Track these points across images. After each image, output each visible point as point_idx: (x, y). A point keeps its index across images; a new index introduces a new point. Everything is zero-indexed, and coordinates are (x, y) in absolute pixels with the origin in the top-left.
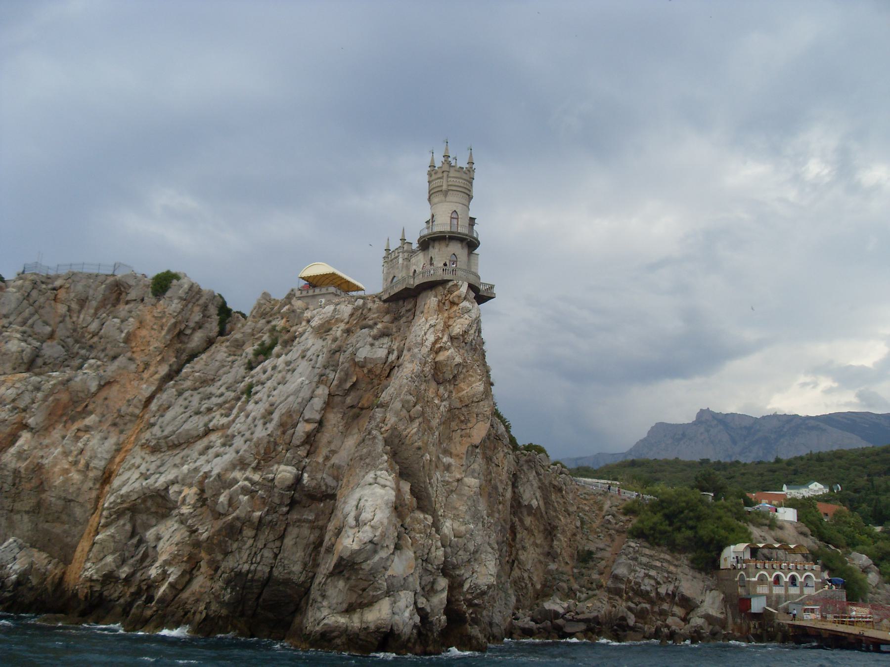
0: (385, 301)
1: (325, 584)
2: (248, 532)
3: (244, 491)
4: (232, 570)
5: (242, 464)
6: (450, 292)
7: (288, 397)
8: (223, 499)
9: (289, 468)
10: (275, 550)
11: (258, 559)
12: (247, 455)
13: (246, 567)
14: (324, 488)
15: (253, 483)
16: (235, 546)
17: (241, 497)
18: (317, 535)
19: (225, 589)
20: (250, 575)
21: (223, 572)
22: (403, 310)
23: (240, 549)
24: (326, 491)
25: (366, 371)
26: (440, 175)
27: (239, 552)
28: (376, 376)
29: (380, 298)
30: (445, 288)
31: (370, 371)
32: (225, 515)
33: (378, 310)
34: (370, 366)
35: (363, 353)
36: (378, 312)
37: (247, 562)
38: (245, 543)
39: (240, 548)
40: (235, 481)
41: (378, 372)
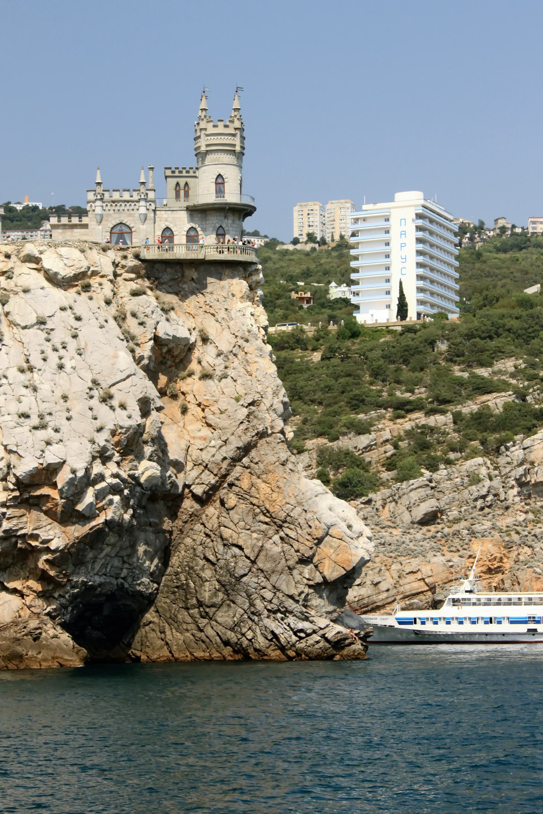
0: (143, 261)
1: (308, 595)
2: (112, 539)
3: (114, 490)
4: (84, 583)
5: (103, 456)
6: (250, 275)
7: (128, 377)
8: (89, 497)
9: (155, 464)
10: (125, 559)
11: (108, 570)
12: (110, 446)
13: (98, 580)
14: (168, 487)
15: (123, 480)
16: (90, 555)
17: (111, 497)
18: (162, 540)
19: (66, 608)
20: (99, 589)
21: (73, 587)
22: (166, 277)
23: (95, 560)
24: (170, 490)
25: (165, 350)
26: (233, 132)
27: (94, 562)
28: (173, 357)
29: (137, 256)
30: (245, 270)
31: (169, 351)
32: (94, 517)
33: (132, 270)
34: (171, 345)
35: (165, 330)
36: (132, 272)
37: (97, 574)
38: (102, 550)
39: (96, 558)
40: (101, 477)
41: (176, 353)
